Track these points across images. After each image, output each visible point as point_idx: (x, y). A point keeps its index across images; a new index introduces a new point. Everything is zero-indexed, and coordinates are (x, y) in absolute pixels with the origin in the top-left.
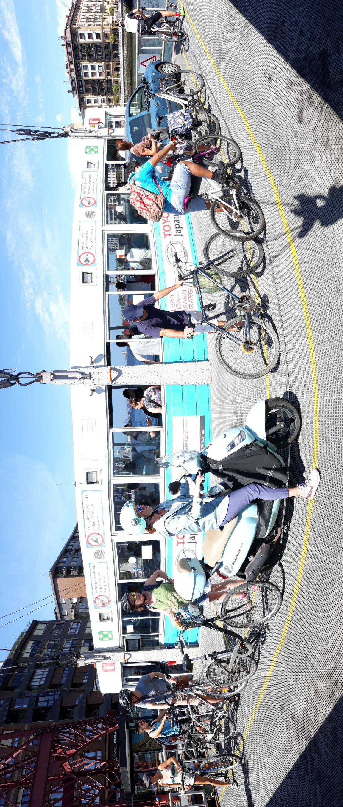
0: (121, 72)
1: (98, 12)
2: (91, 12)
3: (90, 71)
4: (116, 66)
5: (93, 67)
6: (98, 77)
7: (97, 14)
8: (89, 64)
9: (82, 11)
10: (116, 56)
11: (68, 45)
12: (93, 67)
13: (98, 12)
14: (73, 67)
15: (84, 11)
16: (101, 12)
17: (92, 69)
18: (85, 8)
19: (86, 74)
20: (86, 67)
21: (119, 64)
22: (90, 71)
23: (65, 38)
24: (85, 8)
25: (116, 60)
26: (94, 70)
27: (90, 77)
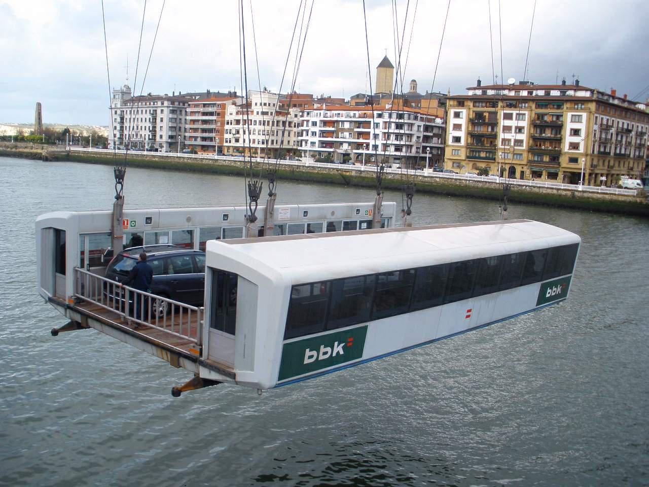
0: (505, 180)
1: (616, 148)
2: (617, 135)
3: (513, 123)
4: (518, 170)
5: (520, 130)
6: (501, 136)
7: (613, 147)
8: (524, 124)
9: (621, 121)
10: (537, 174)
11: (563, 88)
12: (520, 130)
13: (616, 148)
14: (524, 93)
15: (620, 126)
16: (615, 154)
17: (516, 127)
18: (625, 127)
19: (508, 117)
20: (520, 117)
21: (522, 178)
22: (513, 123)
23: (577, 87)
24: (625, 127)
25: (528, 172)
26: (514, 130)
27: (503, 122)
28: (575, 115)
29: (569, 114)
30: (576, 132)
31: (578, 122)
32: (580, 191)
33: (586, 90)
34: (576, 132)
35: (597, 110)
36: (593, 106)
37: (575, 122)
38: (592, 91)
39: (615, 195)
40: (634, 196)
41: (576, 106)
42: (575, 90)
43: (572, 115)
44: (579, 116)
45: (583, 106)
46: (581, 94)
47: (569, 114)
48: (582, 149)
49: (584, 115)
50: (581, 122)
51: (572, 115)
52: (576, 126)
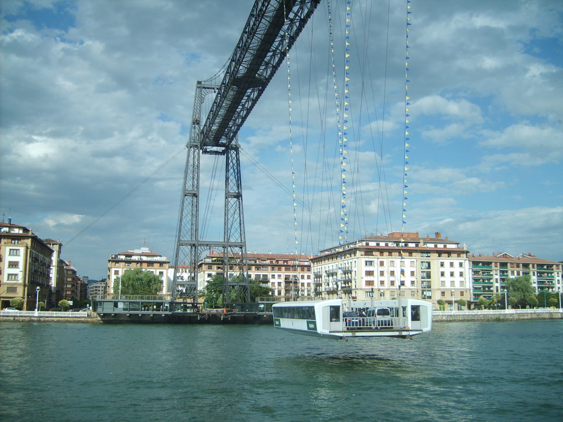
28: (13, 250)
29: (8, 249)
30: (13, 265)
31: (16, 255)
32: (37, 317)
33: (19, 228)
34: (13, 265)
35: (32, 247)
36: (29, 242)
37: (13, 255)
38: (25, 230)
39: (69, 317)
40: (85, 317)
41: (13, 242)
42: (9, 227)
43: (10, 250)
44: (17, 250)
45: (19, 242)
46: (16, 231)
47: (8, 249)
48: (20, 279)
49: (22, 250)
50: (19, 256)
51: (10, 250)
52: (14, 259)
